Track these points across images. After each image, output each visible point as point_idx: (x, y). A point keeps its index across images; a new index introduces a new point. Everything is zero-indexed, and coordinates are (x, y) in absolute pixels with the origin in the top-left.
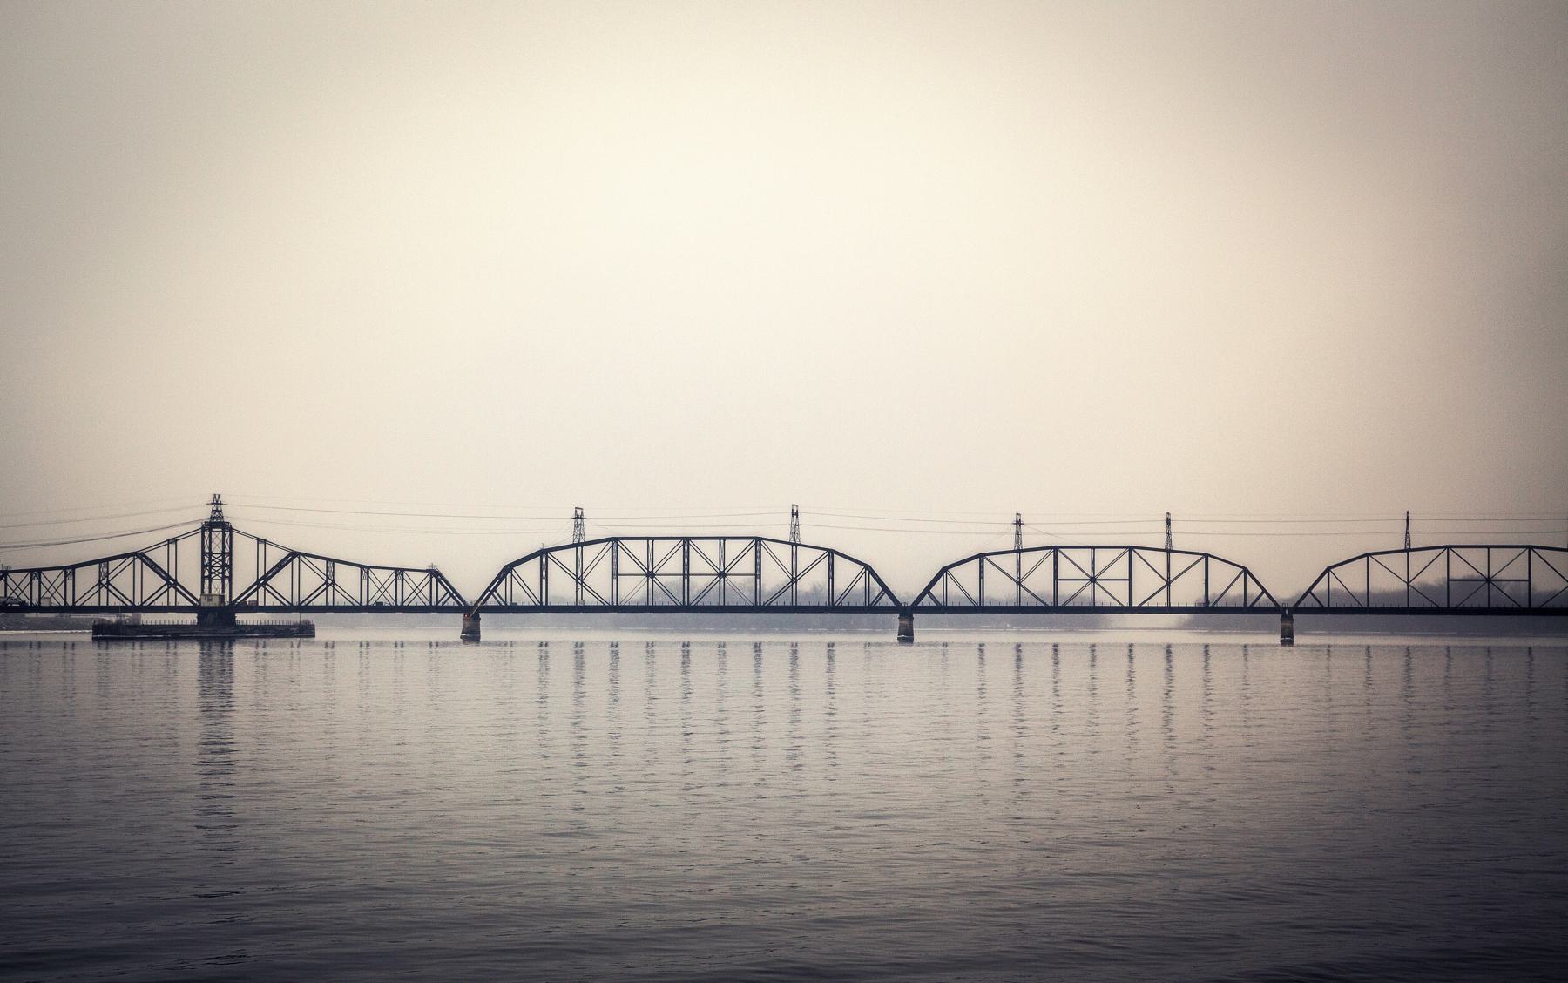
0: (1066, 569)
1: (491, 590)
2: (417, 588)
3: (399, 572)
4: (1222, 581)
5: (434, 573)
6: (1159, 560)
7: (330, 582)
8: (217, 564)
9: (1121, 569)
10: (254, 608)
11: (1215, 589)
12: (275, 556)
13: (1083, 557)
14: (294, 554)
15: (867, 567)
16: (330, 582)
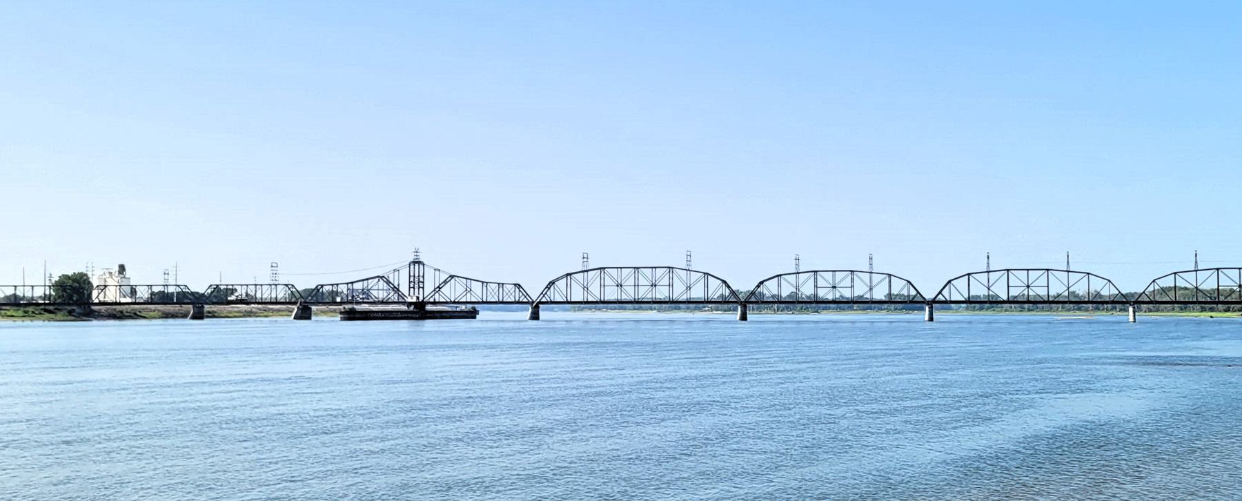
0: (821, 283)
1: (543, 294)
2: (510, 294)
3: (501, 285)
4: (899, 288)
5: (518, 286)
6: (866, 277)
7: (468, 290)
8: (417, 282)
9: (848, 282)
10: (434, 303)
11: (894, 291)
12: (444, 277)
13: (829, 276)
14: (452, 277)
15: (724, 282)
16: (468, 290)
